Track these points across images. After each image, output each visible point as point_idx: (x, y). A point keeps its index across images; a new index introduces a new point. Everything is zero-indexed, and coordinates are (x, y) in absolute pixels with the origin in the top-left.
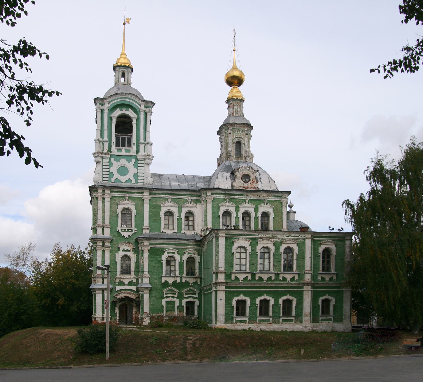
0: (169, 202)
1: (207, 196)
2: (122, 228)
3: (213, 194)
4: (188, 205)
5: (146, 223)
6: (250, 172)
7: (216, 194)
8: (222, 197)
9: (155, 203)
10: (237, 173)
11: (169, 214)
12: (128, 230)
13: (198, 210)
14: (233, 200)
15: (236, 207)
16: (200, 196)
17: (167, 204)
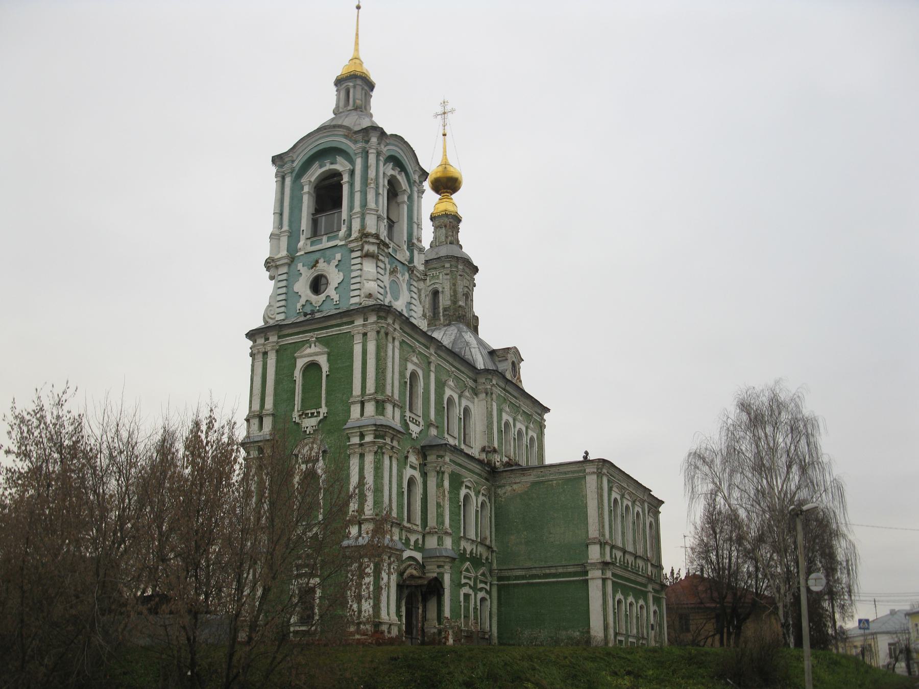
13: (478, 408)
16: (475, 381)
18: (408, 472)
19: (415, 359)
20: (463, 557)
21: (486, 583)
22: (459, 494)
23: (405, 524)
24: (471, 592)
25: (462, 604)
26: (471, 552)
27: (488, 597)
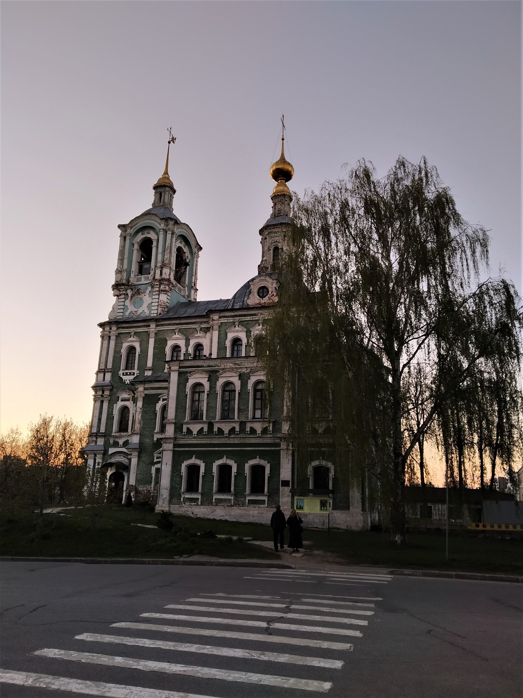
0: (177, 334)
1: (213, 320)
3: (220, 317)
4: (196, 335)
5: (150, 364)
6: (268, 284)
7: (224, 317)
8: (231, 320)
9: (161, 337)
10: (252, 286)
11: (176, 348)
14: (244, 323)
15: (247, 332)
17: (174, 336)
18: (120, 404)
19: (132, 339)
23: (113, 434)
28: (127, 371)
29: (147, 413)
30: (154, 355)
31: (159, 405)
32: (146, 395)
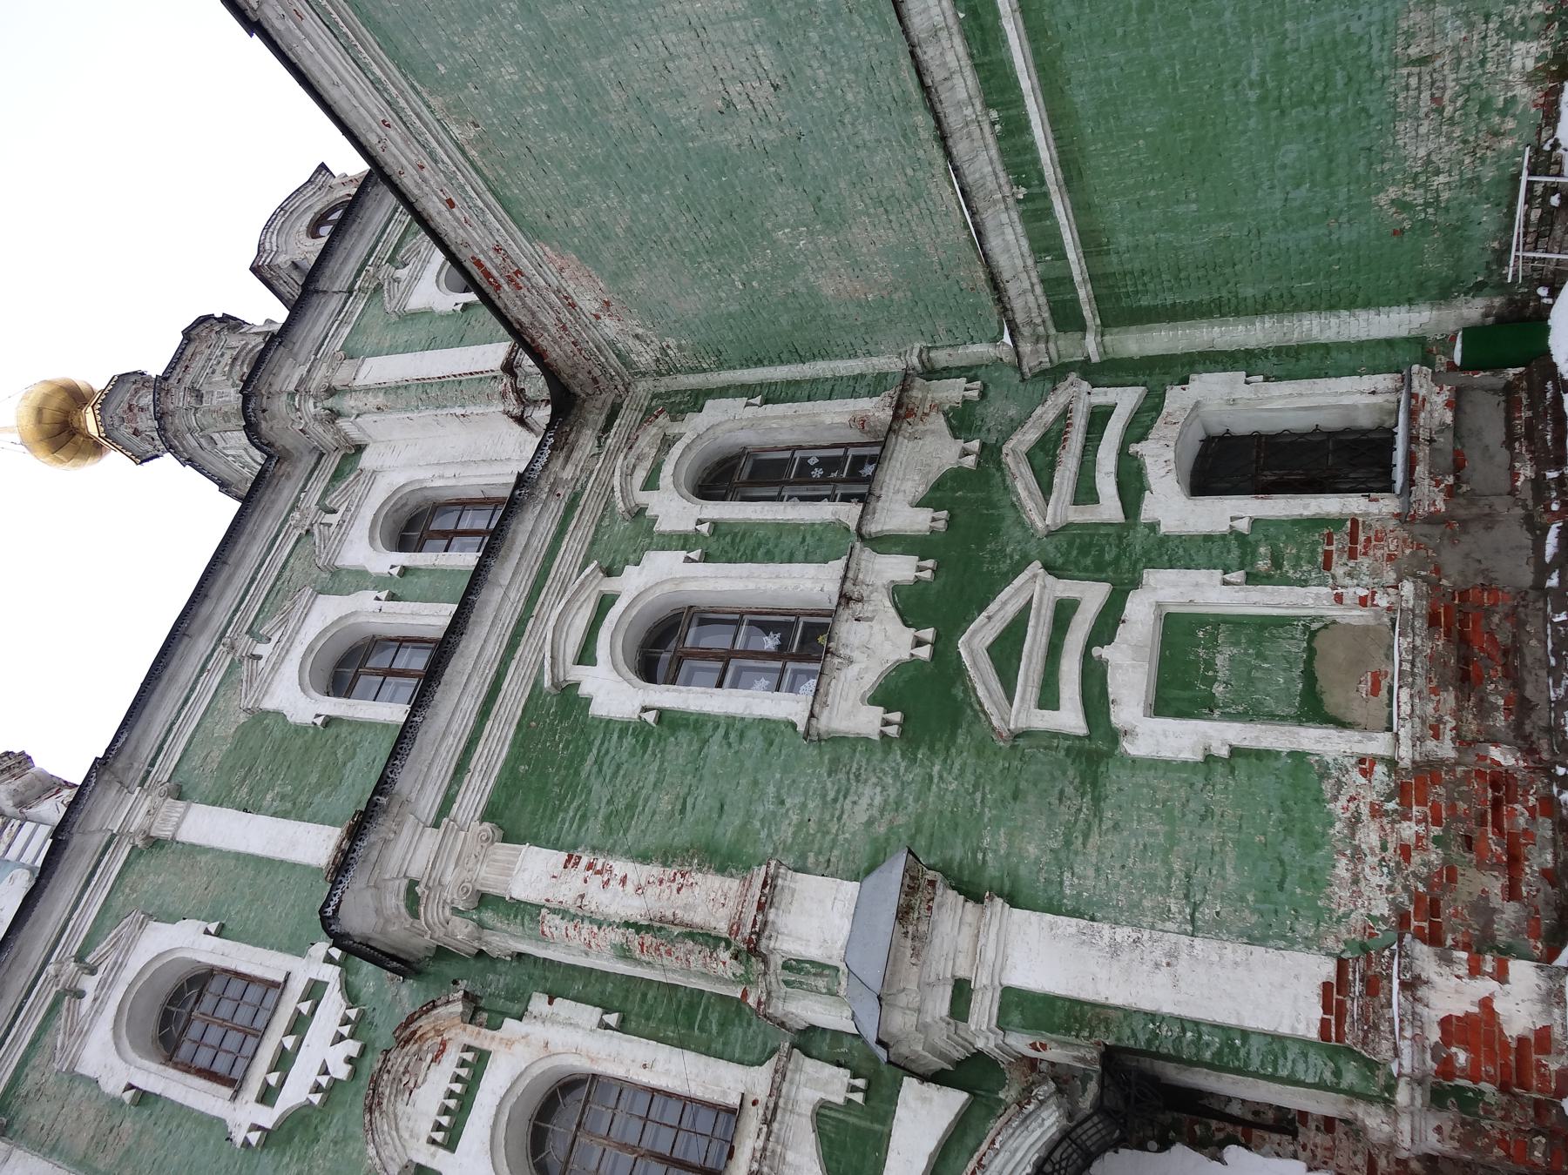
2: (253, 1087)
12: (299, 1025)
20: (926, 701)
21: (1099, 418)
22: (609, 722)
24: (1140, 611)
25: (1222, 734)
26: (910, 605)
27: (1177, 400)
28: (267, 1054)
29: (630, 807)
30: (285, 815)
31: (613, 693)
32: (489, 814)
